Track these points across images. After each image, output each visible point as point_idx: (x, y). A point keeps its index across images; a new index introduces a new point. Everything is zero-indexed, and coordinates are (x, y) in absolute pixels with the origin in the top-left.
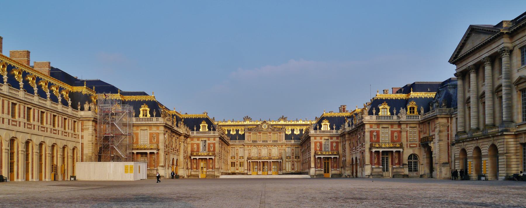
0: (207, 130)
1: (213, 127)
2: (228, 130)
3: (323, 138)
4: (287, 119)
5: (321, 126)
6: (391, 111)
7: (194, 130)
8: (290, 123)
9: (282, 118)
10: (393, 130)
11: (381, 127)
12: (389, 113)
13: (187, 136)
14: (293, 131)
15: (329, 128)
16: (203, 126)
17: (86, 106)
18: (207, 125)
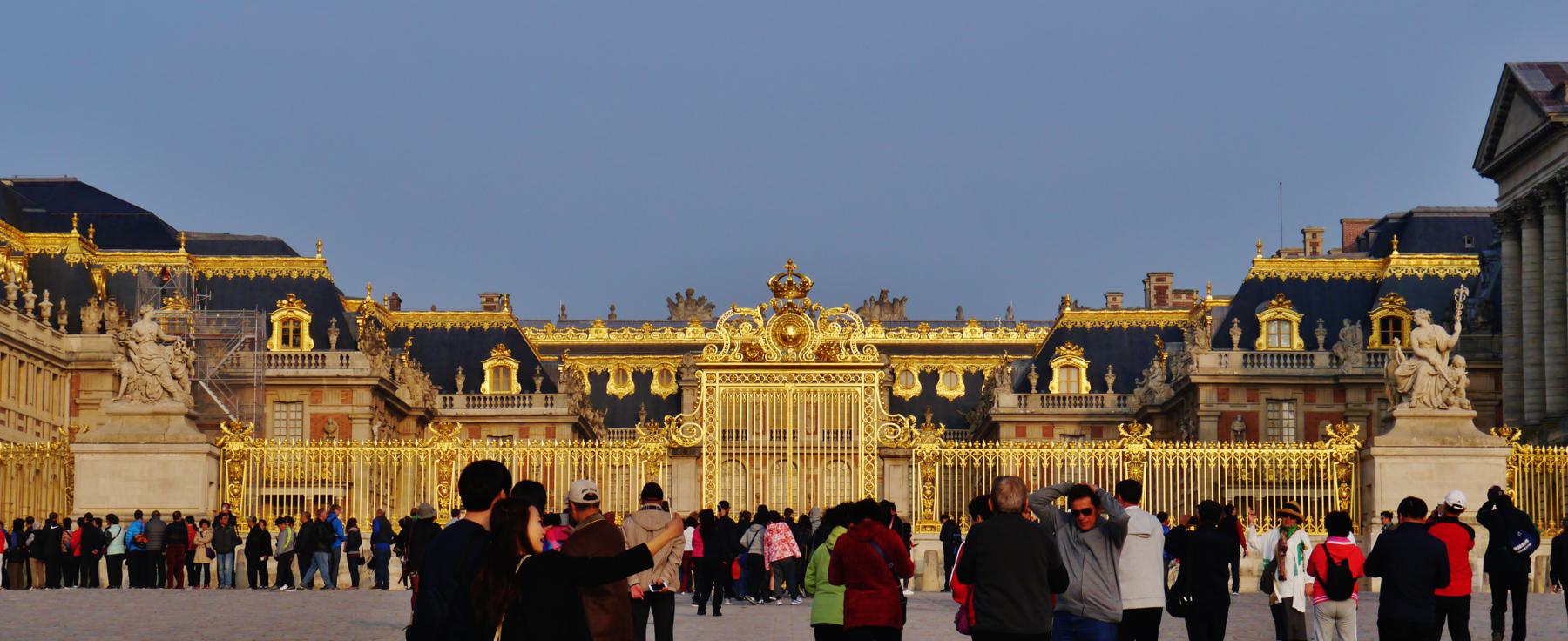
0: (516, 387)
1: (543, 373)
2: (592, 375)
3: (1057, 431)
4: (909, 311)
5: (1046, 375)
6: (1306, 331)
7: (454, 390)
8: (915, 338)
9: (880, 303)
10: (1314, 409)
11: (1262, 397)
12: (1298, 342)
13: (426, 418)
14: (929, 379)
15: (1085, 385)
16: (496, 369)
17: (91, 317)
18: (514, 365)
